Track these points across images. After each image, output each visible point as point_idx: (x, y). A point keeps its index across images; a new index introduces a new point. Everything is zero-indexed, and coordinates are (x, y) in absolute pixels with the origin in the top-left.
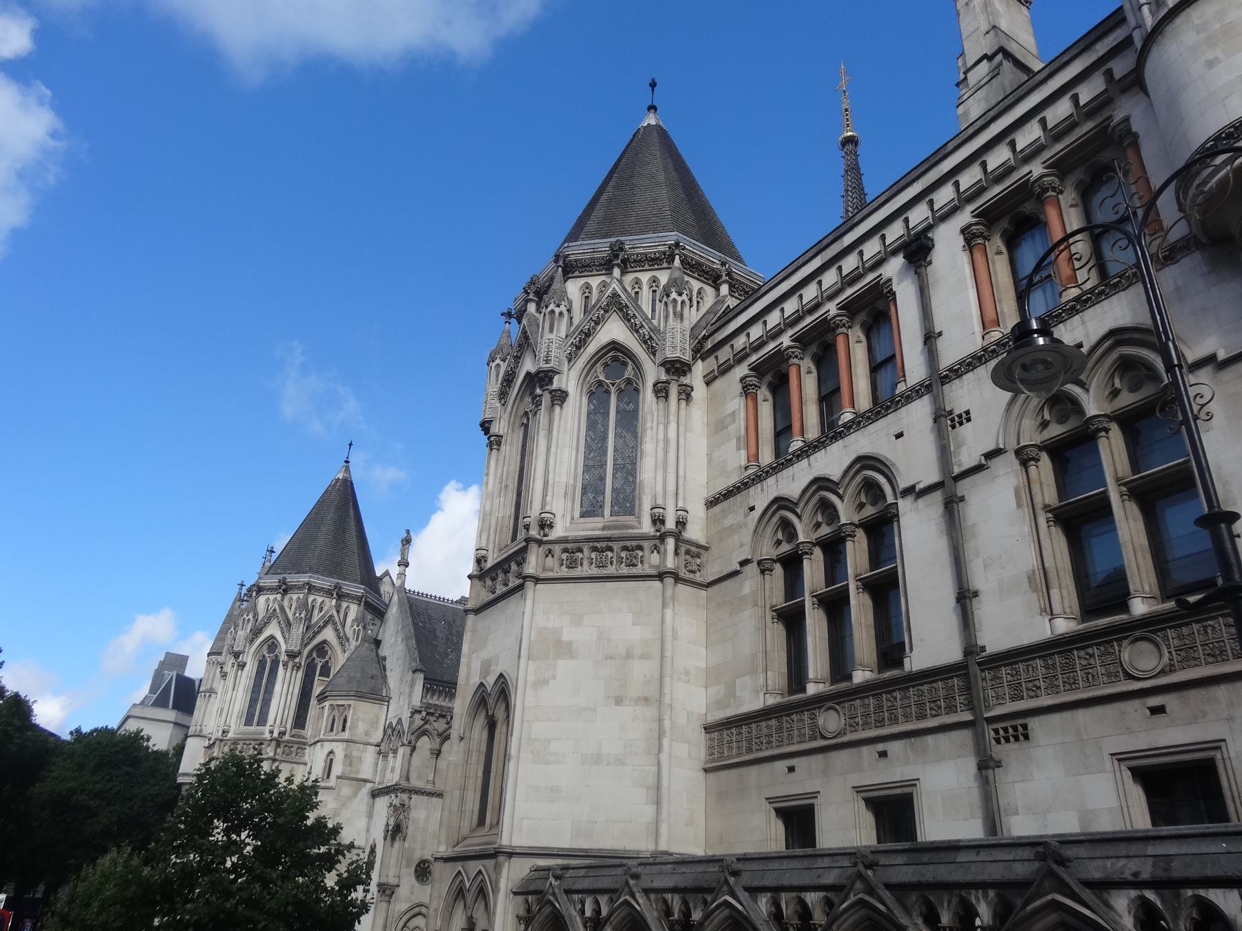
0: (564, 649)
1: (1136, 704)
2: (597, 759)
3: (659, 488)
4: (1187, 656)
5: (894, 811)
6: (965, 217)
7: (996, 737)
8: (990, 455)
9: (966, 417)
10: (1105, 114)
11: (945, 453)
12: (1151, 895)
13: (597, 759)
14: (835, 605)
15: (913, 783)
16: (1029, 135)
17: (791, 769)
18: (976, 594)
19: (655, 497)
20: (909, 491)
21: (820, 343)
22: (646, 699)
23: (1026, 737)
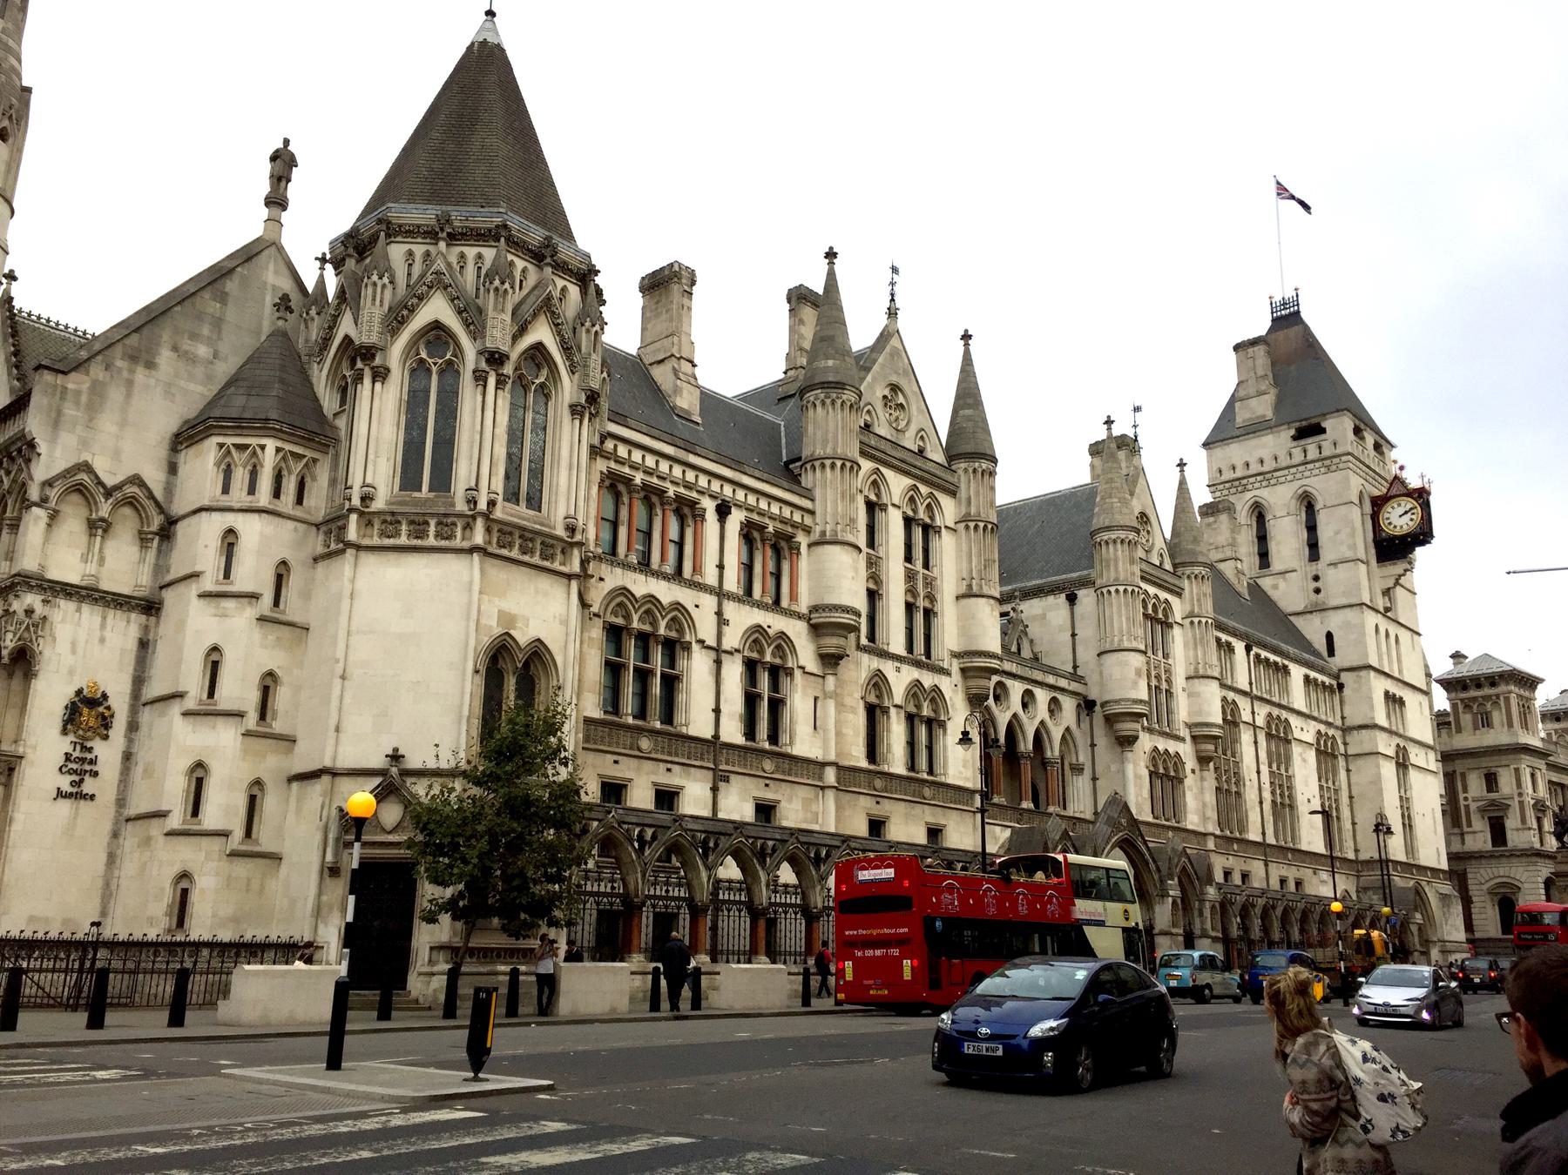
4: (776, 771)
5: (666, 798)
7: (719, 780)
14: (643, 676)
15: (682, 788)
16: (775, 509)
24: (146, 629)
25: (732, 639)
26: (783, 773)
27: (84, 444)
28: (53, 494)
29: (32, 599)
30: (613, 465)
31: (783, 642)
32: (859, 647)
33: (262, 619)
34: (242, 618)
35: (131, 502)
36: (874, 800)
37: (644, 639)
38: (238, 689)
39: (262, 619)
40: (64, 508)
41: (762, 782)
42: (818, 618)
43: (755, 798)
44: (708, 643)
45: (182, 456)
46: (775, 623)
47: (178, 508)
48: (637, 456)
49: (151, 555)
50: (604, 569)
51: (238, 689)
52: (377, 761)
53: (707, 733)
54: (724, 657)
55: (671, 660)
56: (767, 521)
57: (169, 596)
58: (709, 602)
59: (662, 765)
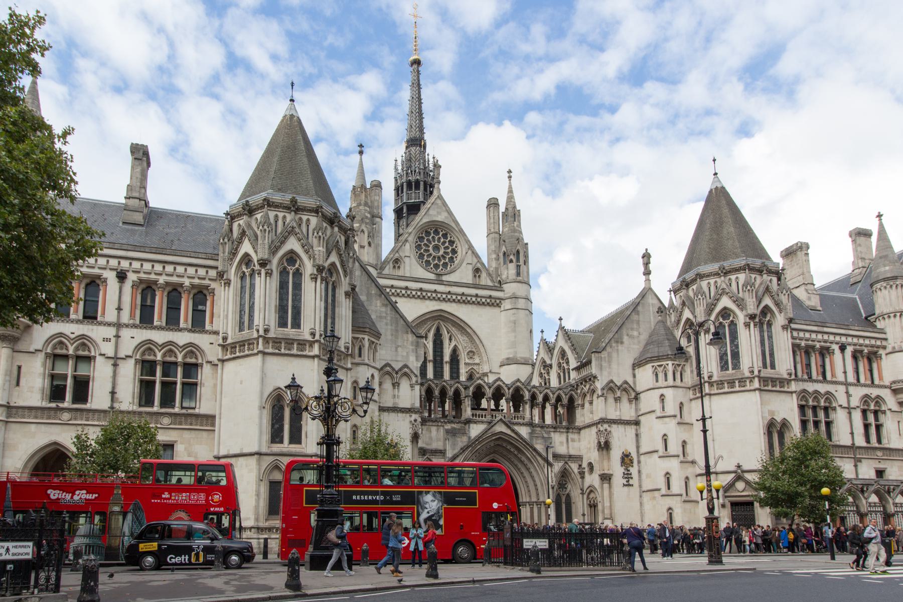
14: (816, 424)
24: (637, 430)
25: (855, 402)
27: (610, 373)
28: (605, 392)
29: (606, 426)
31: (879, 400)
33: (679, 423)
34: (672, 423)
35: (625, 390)
37: (814, 408)
38: (674, 447)
39: (679, 423)
40: (608, 396)
42: (894, 387)
45: (636, 371)
46: (874, 392)
47: (639, 389)
49: (633, 405)
51: (674, 447)
52: (732, 468)
54: (852, 411)
55: (827, 415)
57: (642, 419)
58: (842, 389)
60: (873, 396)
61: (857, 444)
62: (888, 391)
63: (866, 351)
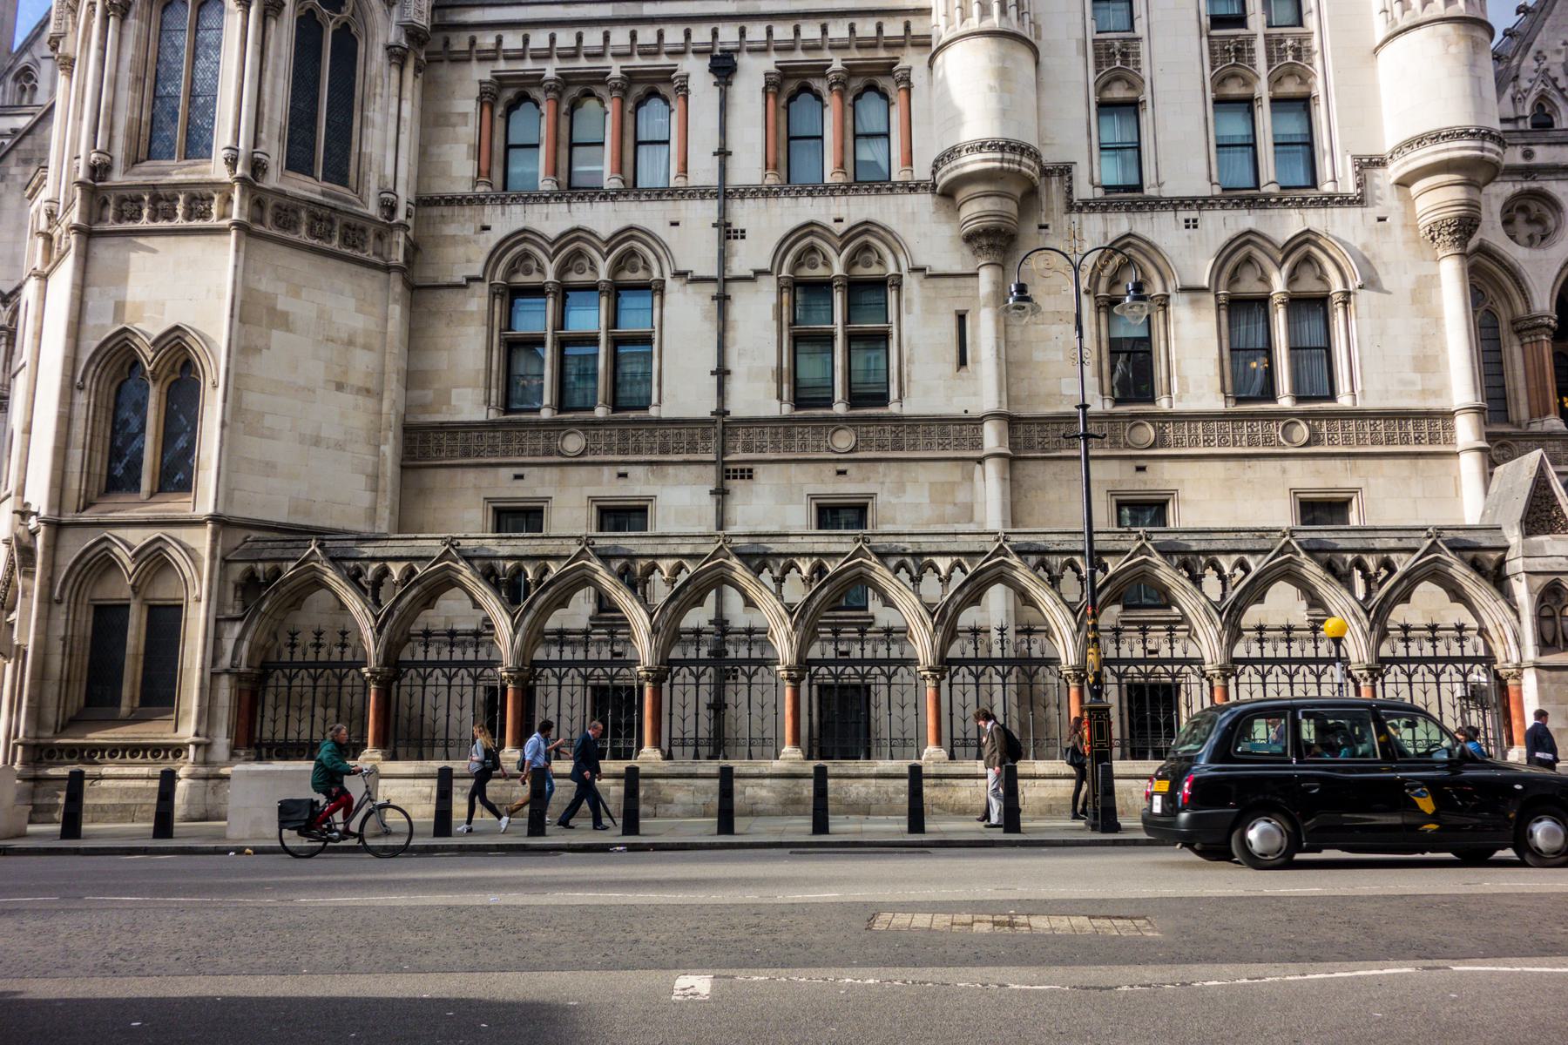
0: (282, 320)
1: (831, 466)
2: (317, 441)
3: (389, 171)
5: (622, 516)
6: (769, 63)
7: (729, 475)
8: (758, 273)
9: (742, 234)
10: (896, 53)
11: (723, 258)
12: (909, 560)
13: (317, 441)
17: (519, 477)
18: (728, 372)
19: (382, 177)
20: (679, 274)
21: (578, 89)
22: (368, 391)
23: (750, 477)
25: (751, 255)
26: (881, 447)
30: (502, 65)
32: (1071, 207)
36: (1130, 466)
41: (829, 470)
43: (812, 497)
44: (700, 272)
48: (540, 39)
50: (491, 214)
53: (703, 407)
54: (734, 290)
56: (827, 54)
59: (606, 469)
60: (840, 229)
61: (739, 407)
62: (923, 203)
63: (837, 65)
